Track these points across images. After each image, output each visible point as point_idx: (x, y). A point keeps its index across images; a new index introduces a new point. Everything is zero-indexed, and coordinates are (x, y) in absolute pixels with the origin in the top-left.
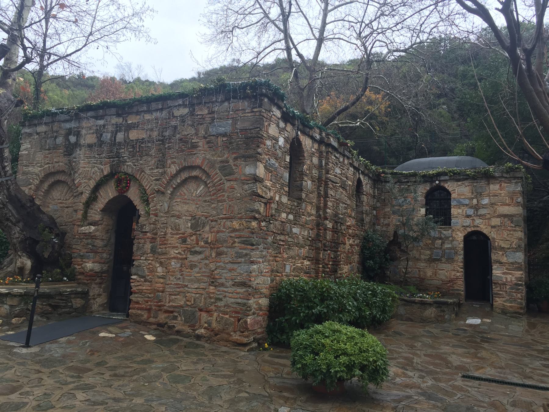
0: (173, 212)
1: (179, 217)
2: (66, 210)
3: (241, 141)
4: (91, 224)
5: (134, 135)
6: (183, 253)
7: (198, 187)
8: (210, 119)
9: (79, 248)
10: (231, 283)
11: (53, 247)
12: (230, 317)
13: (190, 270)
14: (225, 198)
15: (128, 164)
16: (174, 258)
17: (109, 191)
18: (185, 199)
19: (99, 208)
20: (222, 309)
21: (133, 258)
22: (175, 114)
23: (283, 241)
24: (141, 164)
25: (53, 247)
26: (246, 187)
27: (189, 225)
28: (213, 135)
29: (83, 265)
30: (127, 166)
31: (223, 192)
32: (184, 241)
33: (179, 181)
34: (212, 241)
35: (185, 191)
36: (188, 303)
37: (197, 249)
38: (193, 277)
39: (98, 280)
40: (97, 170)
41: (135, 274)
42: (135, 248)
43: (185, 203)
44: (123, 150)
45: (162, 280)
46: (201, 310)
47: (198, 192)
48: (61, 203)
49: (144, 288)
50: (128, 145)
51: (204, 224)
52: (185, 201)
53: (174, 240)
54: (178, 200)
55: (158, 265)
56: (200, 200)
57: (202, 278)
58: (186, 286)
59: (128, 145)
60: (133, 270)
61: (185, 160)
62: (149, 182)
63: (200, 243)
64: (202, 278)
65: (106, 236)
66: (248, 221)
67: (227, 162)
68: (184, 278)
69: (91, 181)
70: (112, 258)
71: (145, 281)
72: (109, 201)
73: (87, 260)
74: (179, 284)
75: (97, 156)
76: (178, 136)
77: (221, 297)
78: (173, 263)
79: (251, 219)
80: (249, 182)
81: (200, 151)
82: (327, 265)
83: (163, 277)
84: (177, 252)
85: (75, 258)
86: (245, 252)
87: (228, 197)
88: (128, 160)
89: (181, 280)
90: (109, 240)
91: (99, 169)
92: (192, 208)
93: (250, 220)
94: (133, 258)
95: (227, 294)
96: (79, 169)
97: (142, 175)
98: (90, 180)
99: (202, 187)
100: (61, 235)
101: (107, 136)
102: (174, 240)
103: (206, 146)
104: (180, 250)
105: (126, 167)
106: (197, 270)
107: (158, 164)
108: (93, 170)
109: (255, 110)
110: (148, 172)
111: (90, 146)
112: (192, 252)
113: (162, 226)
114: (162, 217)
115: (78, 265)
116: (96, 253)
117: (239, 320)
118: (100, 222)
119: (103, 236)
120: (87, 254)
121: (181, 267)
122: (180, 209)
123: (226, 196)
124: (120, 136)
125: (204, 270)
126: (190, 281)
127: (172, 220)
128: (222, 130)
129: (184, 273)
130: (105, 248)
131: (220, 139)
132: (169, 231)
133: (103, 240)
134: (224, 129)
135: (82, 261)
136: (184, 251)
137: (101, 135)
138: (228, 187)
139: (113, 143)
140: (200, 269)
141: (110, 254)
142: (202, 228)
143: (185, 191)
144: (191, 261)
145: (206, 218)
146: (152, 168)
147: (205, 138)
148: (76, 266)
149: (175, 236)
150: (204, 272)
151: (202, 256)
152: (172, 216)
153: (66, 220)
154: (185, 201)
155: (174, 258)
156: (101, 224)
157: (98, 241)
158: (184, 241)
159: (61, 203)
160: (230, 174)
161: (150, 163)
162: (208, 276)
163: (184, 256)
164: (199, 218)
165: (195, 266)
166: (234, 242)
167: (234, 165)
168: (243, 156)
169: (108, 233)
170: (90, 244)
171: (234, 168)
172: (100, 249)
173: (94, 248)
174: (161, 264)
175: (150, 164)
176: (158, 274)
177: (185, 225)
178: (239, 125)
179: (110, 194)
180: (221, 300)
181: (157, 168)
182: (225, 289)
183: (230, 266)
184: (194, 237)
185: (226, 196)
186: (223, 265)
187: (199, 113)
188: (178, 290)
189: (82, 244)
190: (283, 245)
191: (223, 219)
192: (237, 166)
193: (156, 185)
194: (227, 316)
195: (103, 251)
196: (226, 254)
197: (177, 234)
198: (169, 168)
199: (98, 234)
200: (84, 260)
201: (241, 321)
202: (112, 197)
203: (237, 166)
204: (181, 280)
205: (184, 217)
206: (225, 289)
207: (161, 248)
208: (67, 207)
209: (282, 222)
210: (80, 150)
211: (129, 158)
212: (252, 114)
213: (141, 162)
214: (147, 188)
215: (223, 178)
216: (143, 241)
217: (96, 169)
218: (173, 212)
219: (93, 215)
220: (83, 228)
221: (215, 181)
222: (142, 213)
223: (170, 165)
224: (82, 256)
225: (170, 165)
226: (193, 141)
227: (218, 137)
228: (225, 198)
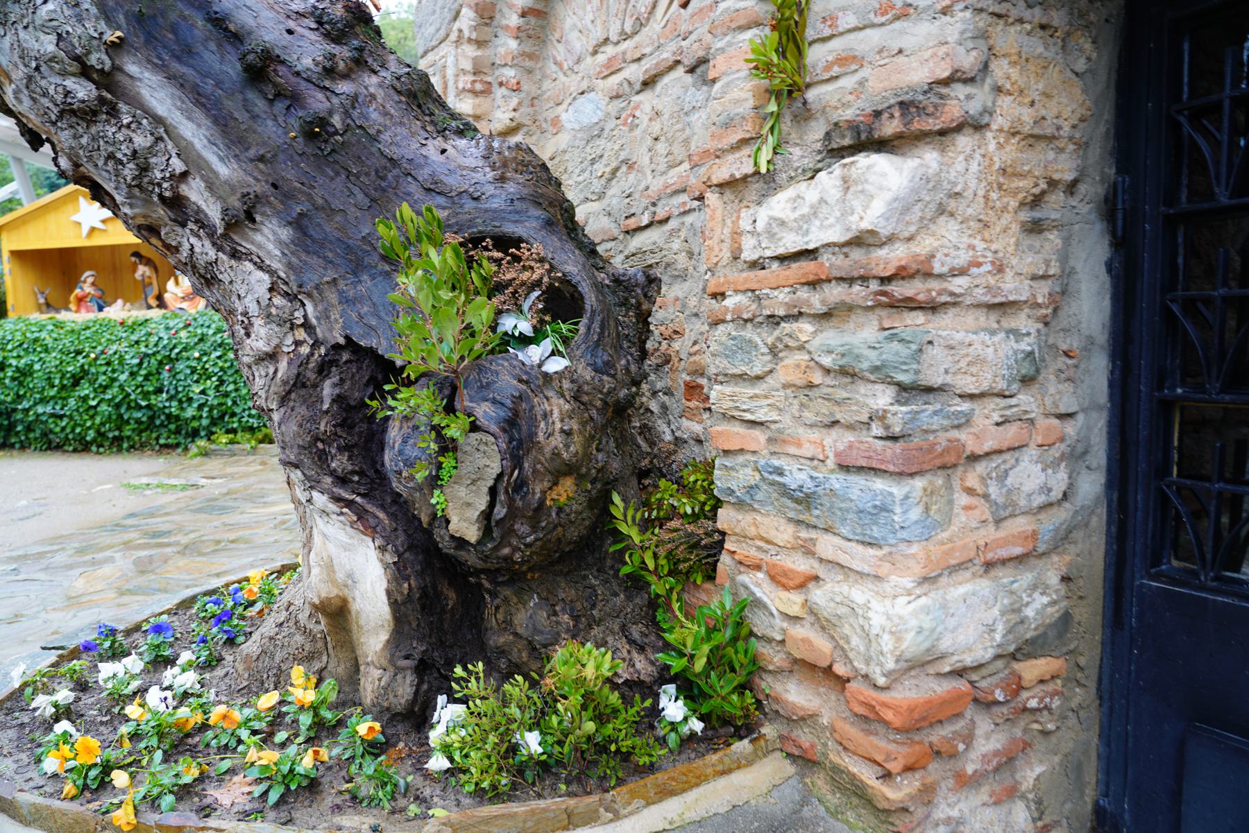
2: (647, 100)
4: (865, 140)
9: (760, 416)
11: (517, 431)
25: (517, 431)
29: (818, 595)
39: (988, 739)
48: (611, 70)
65: (1030, 262)
70: (1092, 485)
73: (860, 557)
90: (1063, 294)
100: (613, 310)
115: (779, 578)
116: (951, 462)
118: (962, 102)
119: (1000, 269)
120: (859, 489)
130: (1026, 400)
133: (1003, 307)
135: (808, 550)
141: (1076, 457)
148: (758, 585)
153: (656, 184)
156: (977, 126)
157: (947, 327)
159: (611, 70)
169: (1035, 228)
170: (881, 374)
172: (989, 412)
173: (928, 412)
189: (791, 367)
195: (1011, 433)
199: (948, 243)
200: (827, 545)
208: (648, 84)
220: (779, 204)
224: (806, 500)
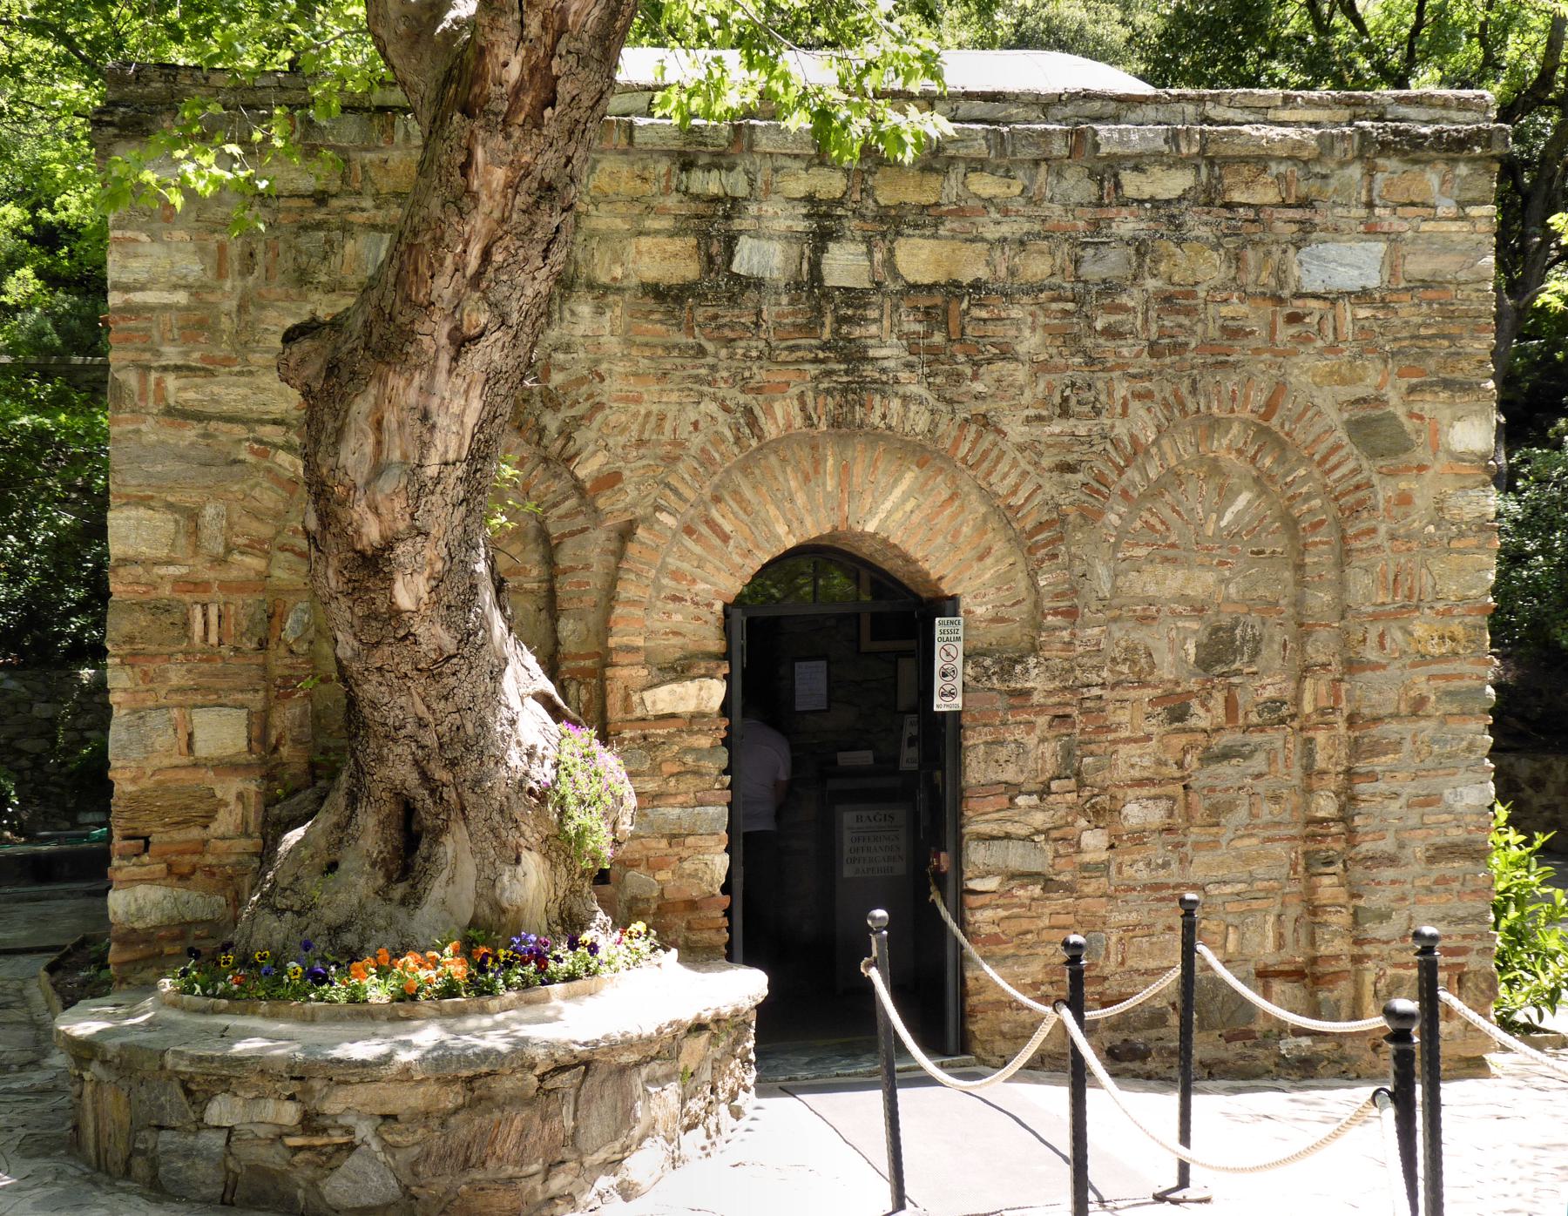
0: (1116, 602)
1: (1145, 620)
3: (1427, 326)
5: (919, 259)
7: (1226, 495)
8: (1294, 227)
10: (1419, 850)
16: (1140, 783)
17: (773, 511)
18: (1173, 546)
19: (718, 594)
22: (1130, 190)
24: (978, 397)
27: (1192, 650)
28: (1315, 296)
32: (1178, 714)
33: (1153, 475)
34: (1316, 710)
35: (1167, 513)
40: (722, 417)
41: (988, 874)
43: (1174, 561)
44: (873, 329)
47: (1228, 516)
49: (1046, 922)
50: (896, 307)
51: (1257, 641)
52: (1171, 553)
53: (1131, 715)
54: (1141, 552)
55: (1082, 822)
56: (1233, 550)
59: (896, 307)
60: (977, 855)
61: (1194, 390)
62: (1025, 473)
63: (1241, 714)
67: (1379, 401)
69: (681, 466)
74: (1167, 886)
76: (1151, 284)
80: (1469, 482)
81: (1257, 351)
83: (1102, 868)
84: (1147, 762)
87: (1393, 537)
88: (904, 376)
89: (1175, 866)
91: (727, 410)
92: (1201, 583)
96: (599, 406)
97: (985, 444)
101: (763, 255)
102: (1131, 715)
105: (896, 404)
107: (1065, 400)
108: (693, 416)
109: (1474, 211)
110: (1016, 431)
111: (657, 292)
121: (1171, 814)
122: (1152, 590)
124: (845, 264)
125: (1267, 818)
128: (1347, 278)
129: (1181, 838)
131: (1346, 311)
134: (1356, 273)
137: (730, 241)
138: (1388, 500)
139: (810, 284)
140: (1253, 815)
142: (1251, 662)
143: (1167, 513)
144: (1212, 789)
146: (1039, 418)
147: (1279, 300)
149: (1133, 694)
150: (1279, 824)
151: (1258, 763)
152: (1115, 620)
154: (1171, 553)
155: (1140, 783)
158: (1178, 714)
161: (1028, 393)
162: (1292, 838)
163: (1177, 774)
164: (1237, 620)
165: (1231, 806)
167: (1411, 415)
168: (1447, 384)
171: (1409, 425)
174: (1101, 813)
175: (1027, 397)
176: (1087, 858)
177: (1174, 652)
178: (1418, 265)
179: (781, 529)
180: (1384, 916)
187: (1237, 196)
193: (1067, 487)
196: (1396, 752)
197: (1143, 684)
202: (791, 542)
203: (1421, 418)
204: (1175, 866)
210: (599, 311)
211: (909, 366)
212: (1465, 226)
213: (979, 387)
217: (713, 408)
219: (689, 627)
221: (1337, 474)
222: (980, 611)
223: (1125, 405)
225: (1125, 405)
226: (1225, 311)
227: (1334, 302)
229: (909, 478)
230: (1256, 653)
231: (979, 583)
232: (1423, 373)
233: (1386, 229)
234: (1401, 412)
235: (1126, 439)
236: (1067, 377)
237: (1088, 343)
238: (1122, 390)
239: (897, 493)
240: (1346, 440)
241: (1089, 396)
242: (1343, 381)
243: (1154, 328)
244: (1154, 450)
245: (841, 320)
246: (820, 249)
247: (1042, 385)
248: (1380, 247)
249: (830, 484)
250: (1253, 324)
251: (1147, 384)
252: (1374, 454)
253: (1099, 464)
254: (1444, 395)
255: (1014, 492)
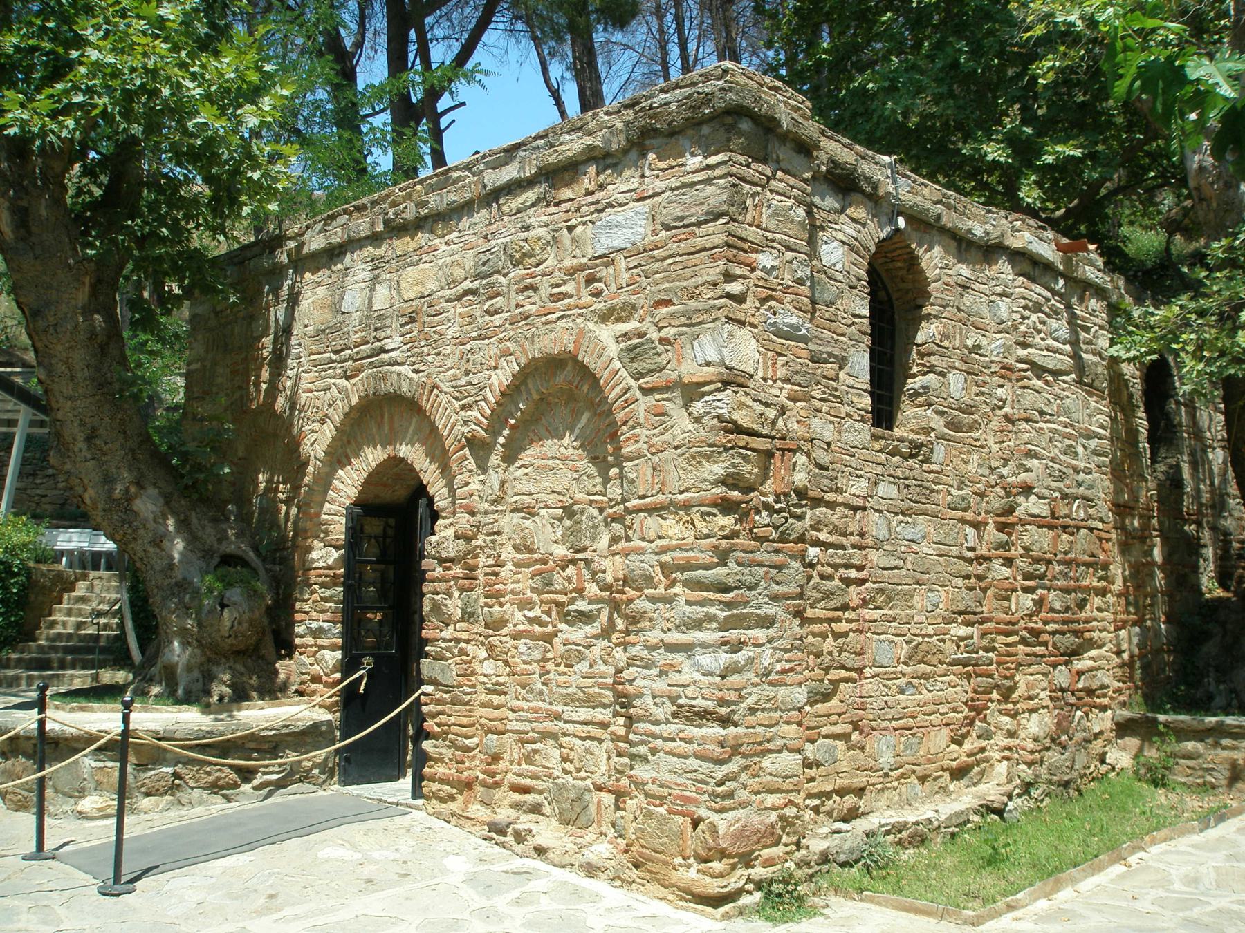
0: (515, 498)
6: (545, 618)
10: (669, 708)
12: (669, 812)
13: (566, 669)
14: (642, 445)
15: (396, 368)
20: (649, 787)
21: (424, 633)
23: (860, 568)
26: (698, 407)
27: (559, 532)
30: (399, 374)
31: (633, 428)
36: (567, 766)
37: (582, 605)
38: (572, 690)
42: (426, 608)
45: (497, 700)
46: (599, 789)
49: (453, 719)
51: (595, 527)
57: (596, 690)
58: (558, 717)
60: (427, 667)
64: (596, 690)
66: (709, 514)
68: (551, 691)
71: (453, 702)
72: (370, 475)
75: (334, 357)
77: (643, 749)
78: (523, 648)
79: (715, 505)
82: (1036, 633)
85: (302, 636)
86: (700, 611)
93: (715, 510)
94: (424, 633)
95: (659, 742)
97: (432, 397)
98: (322, 422)
99: (586, 416)
101: (353, 300)
103: (585, 292)
104: (537, 612)
105: (395, 377)
106: (583, 667)
112: (568, 613)
113: (488, 539)
114: (486, 513)
117: (695, 823)
123: (643, 439)
124: (382, 296)
126: (569, 700)
127: (515, 521)
132: (508, 553)
136: (548, 613)
140: (591, 666)
145: (601, 510)
160: (650, 372)
163: (550, 629)
164: (582, 511)
165: (581, 657)
166: (673, 583)
180: (645, 759)
181: (467, 373)
182: (655, 729)
183: (661, 657)
184: (571, 570)
185: (643, 439)
186: (644, 653)
188: (539, 726)
190: (862, 582)
191: (638, 510)
192: (669, 343)
194: (662, 810)
198: (496, 368)
201: (701, 826)
202: (374, 464)
205: (543, 512)
206: (655, 729)
207: (487, 605)
209: (855, 509)
213: (429, 358)
214: (446, 433)
215: (632, 382)
216: (440, 586)
218: (515, 498)
228: (642, 445)
229: (414, 420)
230: (593, 539)
231: (438, 490)
232: (667, 303)
233: (650, 193)
234: (655, 336)
235: (496, 383)
236: (468, 347)
237: (480, 320)
238: (494, 351)
239: (410, 431)
240: (618, 365)
241: (478, 357)
242: (619, 319)
243: (513, 303)
244: (523, 388)
245: (376, 330)
246: (372, 290)
247: (457, 352)
248: (642, 207)
249: (386, 428)
250: (568, 288)
251: (508, 344)
252: (638, 376)
253: (482, 403)
254: (683, 319)
255: (445, 427)
